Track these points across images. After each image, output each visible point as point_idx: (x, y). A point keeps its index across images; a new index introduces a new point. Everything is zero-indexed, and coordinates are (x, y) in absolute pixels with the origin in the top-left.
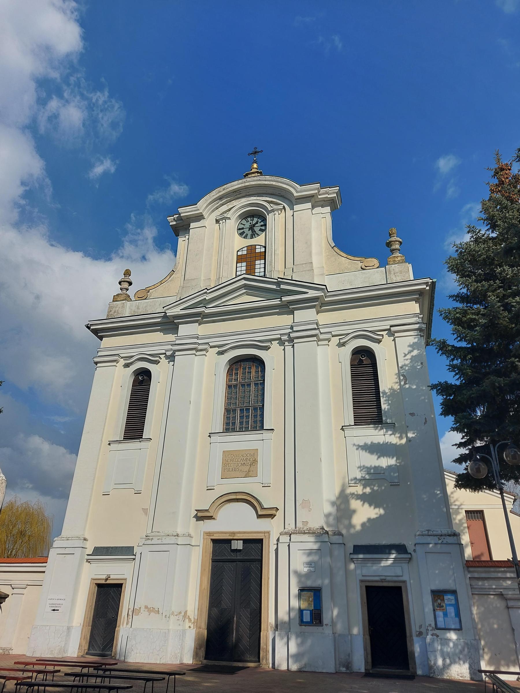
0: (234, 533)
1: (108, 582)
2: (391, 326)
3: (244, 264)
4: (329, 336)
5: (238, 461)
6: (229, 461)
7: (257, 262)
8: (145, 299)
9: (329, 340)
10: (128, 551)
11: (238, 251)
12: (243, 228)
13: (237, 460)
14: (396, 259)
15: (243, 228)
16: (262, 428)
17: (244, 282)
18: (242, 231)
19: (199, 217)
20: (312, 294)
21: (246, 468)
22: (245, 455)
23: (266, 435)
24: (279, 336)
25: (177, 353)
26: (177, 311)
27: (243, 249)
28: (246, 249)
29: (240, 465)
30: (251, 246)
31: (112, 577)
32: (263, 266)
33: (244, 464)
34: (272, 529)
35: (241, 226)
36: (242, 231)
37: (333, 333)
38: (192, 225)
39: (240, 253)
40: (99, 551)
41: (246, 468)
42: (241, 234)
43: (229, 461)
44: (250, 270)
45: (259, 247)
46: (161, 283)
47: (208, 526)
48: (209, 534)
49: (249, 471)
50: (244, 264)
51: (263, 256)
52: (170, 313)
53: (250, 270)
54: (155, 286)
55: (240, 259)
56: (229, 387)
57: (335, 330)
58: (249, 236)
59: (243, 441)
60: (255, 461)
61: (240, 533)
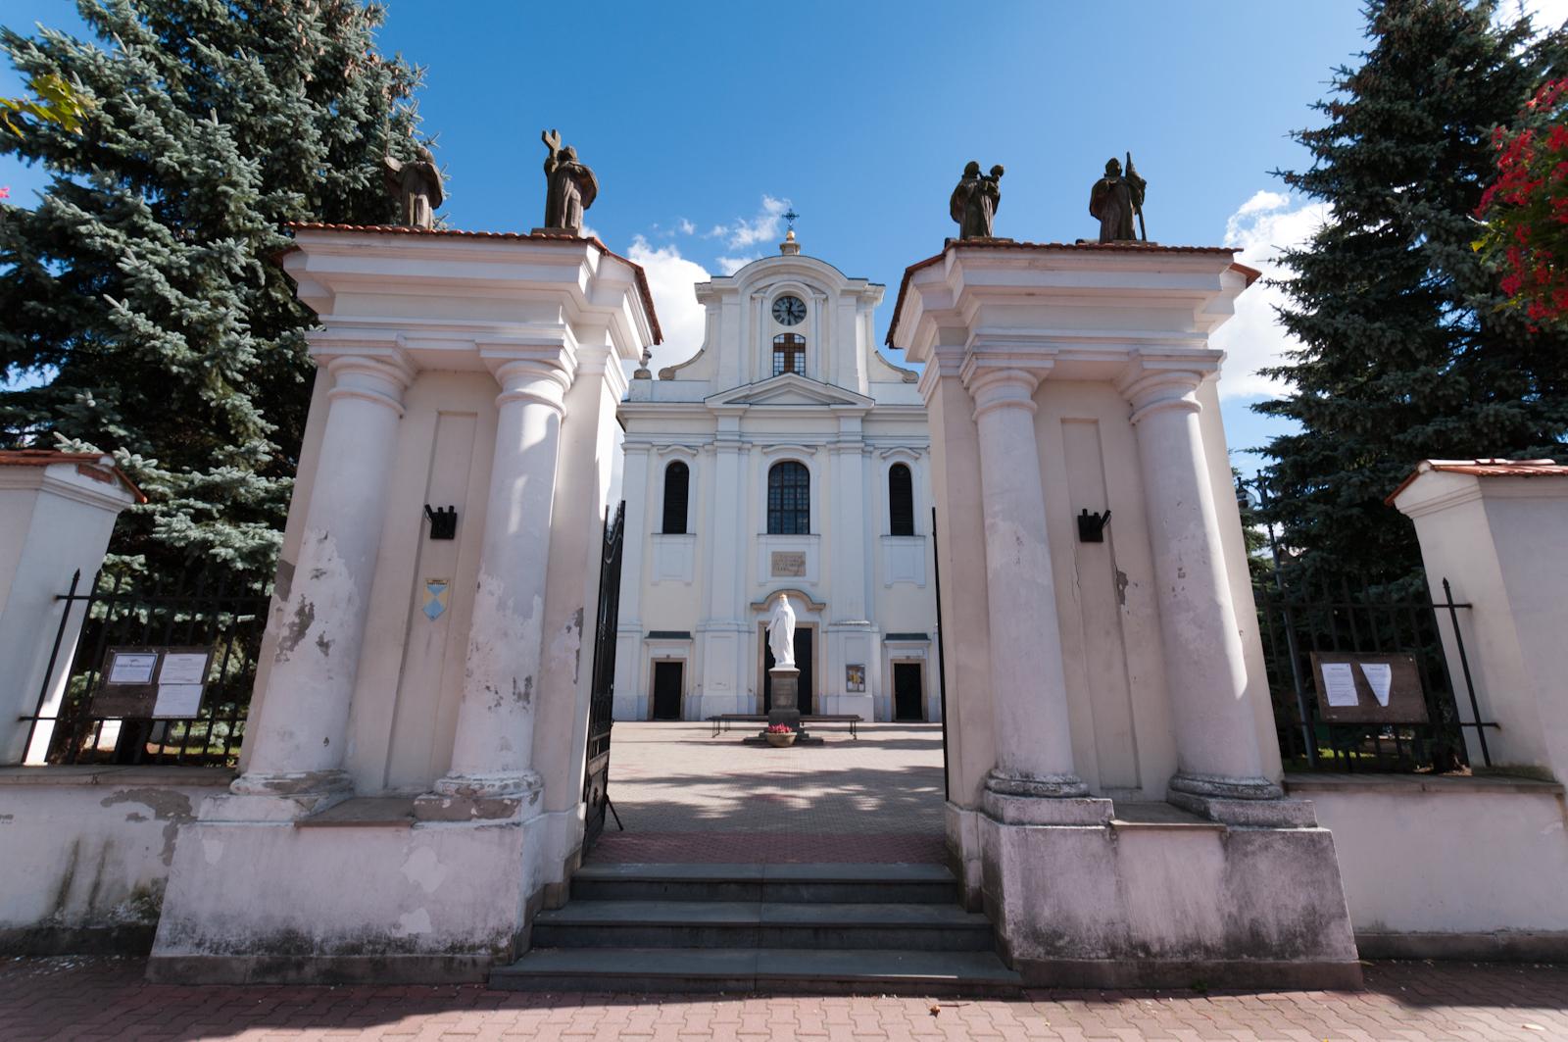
3: (782, 354)
4: (871, 449)
7: (797, 355)
9: (871, 452)
10: (685, 635)
16: (809, 533)
17: (788, 381)
19: (734, 291)
21: (796, 568)
23: (812, 539)
26: (717, 403)
33: (792, 564)
35: (777, 308)
38: (725, 299)
39: (777, 341)
40: (654, 635)
41: (796, 568)
42: (777, 318)
44: (789, 366)
46: (689, 363)
47: (763, 617)
50: (782, 354)
51: (802, 348)
52: (710, 404)
54: (682, 366)
55: (777, 348)
56: (770, 487)
57: (879, 443)
58: (786, 322)
59: (788, 543)
60: (803, 563)
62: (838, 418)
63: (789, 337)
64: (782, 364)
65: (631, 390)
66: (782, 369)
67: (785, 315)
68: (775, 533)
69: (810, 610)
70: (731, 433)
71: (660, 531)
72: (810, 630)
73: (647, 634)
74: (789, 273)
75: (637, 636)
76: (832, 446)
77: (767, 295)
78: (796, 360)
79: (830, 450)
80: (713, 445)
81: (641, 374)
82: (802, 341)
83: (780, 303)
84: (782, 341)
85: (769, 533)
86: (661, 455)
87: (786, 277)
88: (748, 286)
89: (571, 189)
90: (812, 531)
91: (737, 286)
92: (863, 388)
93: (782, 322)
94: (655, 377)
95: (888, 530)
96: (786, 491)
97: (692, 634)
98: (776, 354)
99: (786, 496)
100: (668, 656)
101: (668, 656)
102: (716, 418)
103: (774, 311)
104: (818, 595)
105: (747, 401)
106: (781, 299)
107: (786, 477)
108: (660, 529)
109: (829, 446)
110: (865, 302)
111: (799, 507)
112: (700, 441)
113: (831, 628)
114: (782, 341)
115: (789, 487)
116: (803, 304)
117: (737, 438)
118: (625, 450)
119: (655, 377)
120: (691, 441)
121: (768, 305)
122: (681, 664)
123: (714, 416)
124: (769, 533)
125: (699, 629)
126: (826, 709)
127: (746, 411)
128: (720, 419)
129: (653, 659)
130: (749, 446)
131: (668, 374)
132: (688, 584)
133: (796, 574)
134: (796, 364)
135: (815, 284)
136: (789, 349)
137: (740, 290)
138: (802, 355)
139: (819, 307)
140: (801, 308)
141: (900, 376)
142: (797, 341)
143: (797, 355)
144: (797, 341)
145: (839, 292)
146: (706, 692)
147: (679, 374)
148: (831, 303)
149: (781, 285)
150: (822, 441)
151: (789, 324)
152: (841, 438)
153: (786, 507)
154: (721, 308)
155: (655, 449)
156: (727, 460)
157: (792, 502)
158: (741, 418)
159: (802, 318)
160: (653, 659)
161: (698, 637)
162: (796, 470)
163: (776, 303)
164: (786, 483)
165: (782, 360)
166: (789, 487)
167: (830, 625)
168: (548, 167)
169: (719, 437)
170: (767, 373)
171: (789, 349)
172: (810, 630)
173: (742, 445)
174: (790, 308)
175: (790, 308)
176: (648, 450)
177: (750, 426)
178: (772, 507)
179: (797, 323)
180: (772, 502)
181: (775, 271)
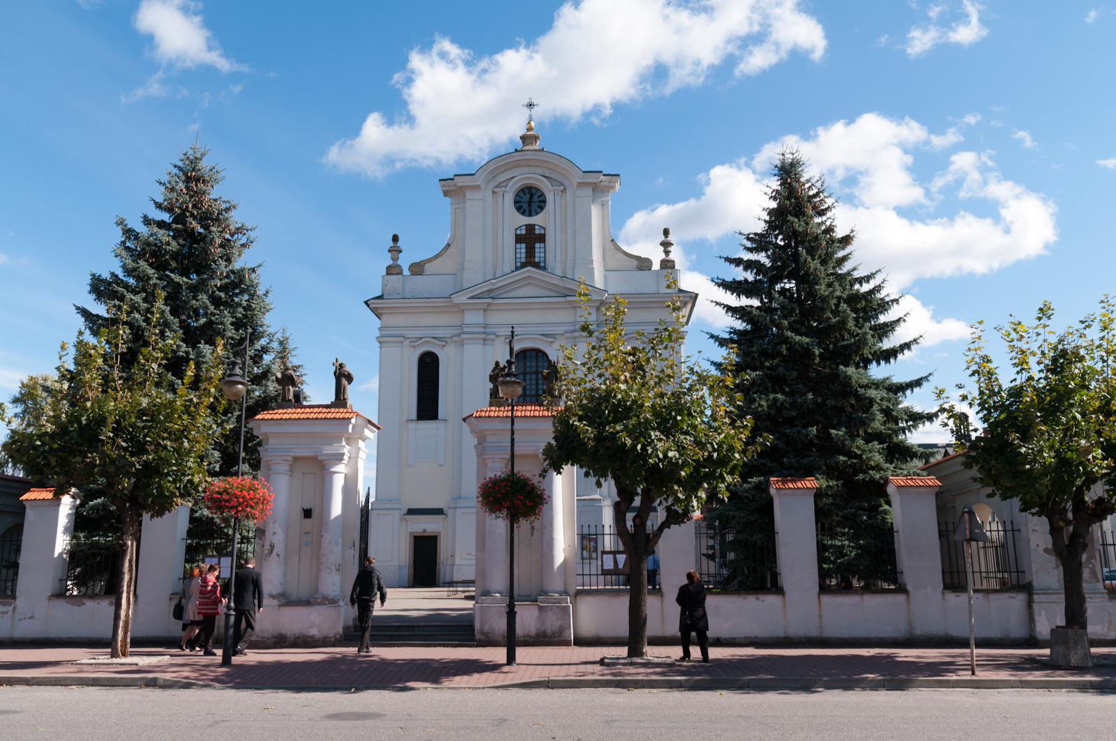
1: (426, 534)
3: (523, 245)
7: (537, 245)
8: (420, 274)
10: (439, 512)
12: (520, 202)
15: (520, 202)
19: (477, 187)
26: (462, 299)
28: (524, 228)
30: (530, 225)
32: (542, 250)
35: (518, 199)
38: (469, 195)
39: (518, 232)
40: (411, 512)
44: (530, 252)
46: (436, 257)
50: (523, 245)
51: (542, 238)
53: (530, 252)
54: (430, 260)
55: (519, 239)
63: (530, 228)
64: (524, 255)
65: (384, 286)
66: (523, 260)
70: (476, 325)
71: (414, 417)
74: (528, 166)
75: (397, 514)
76: (569, 335)
77: (507, 189)
78: (537, 250)
79: (567, 338)
80: (460, 336)
81: (392, 270)
82: (542, 232)
84: (524, 232)
87: (526, 170)
88: (489, 181)
89: (344, 382)
93: (523, 213)
94: (406, 272)
97: (445, 512)
98: (518, 246)
100: (425, 531)
101: (425, 531)
102: (463, 311)
105: (489, 297)
107: (528, 364)
108: (414, 415)
112: (448, 333)
114: (524, 232)
115: (531, 373)
117: (482, 330)
118: (380, 343)
119: (406, 272)
120: (440, 333)
121: (510, 198)
123: (461, 309)
125: (451, 506)
126: (452, 576)
127: (489, 304)
128: (466, 312)
129: (411, 533)
130: (493, 337)
131: (417, 269)
132: (441, 466)
134: (537, 255)
135: (554, 176)
136: (530, 239)
137: (482, 186)
138: (542, 245)
139: (558, 198)
141: (635, 263)
142: (537, 232)
143: (537, 245)
144: (537, 232)
145: (575, 185)
146: (458, 561)
148: (569, 195)
151: (530, 215)
154: (465, 202)
155: (407, 342)
157: (534, 387)
158: (485, 310)
161: (450, 512)
162: (537, 357)
164: (528, 370)
165: (524, 251)
166: (531, 373)
168: (335, 374)
169: (465, 330)
170: (509, 265)
171: (530, 239)
173: (486, 336)
174: (530, 200)
175: (530, 200)
176: (402, 343)
177: (495, 318)
181: (516, 165)
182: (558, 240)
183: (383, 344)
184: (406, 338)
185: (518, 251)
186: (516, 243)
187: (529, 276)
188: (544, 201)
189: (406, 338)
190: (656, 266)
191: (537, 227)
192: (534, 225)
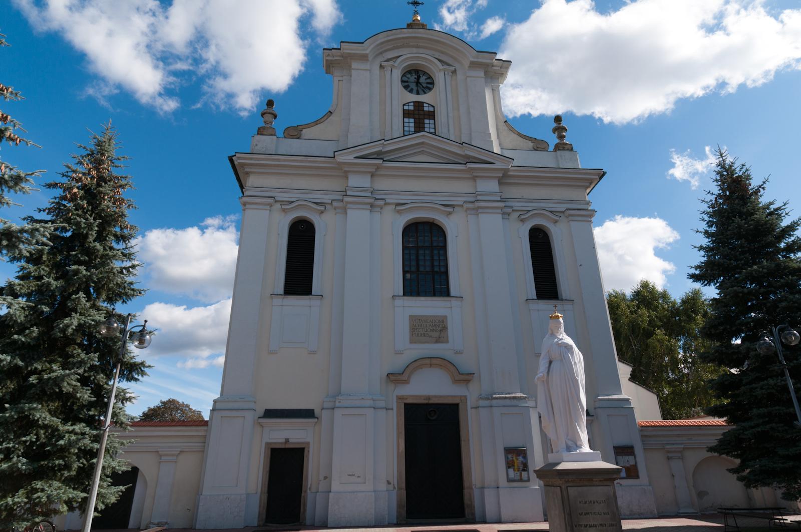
0: (429, 398)
1: (287, 446)
2: (568, 209)
3: (412, 120)
5: (426, 327)
6: (417, 326)
7: (426, 121)
8: (298, 138)
10: (308, 414)
11: (404, 105)
12: (407, 82)
13: (425, 326)
14: (566, 147)
15: (407, 82)
18: (406, 84)
19: (363, 58)
20: (498, 165)
21: (436, 334)
22: (434, 322)
23: (454, 302)
24: (461, 203)
25: (349, 206)
27: (410, 104)
28: (412, 104)
29: (429, 330)
30: (418, 102)
31: (290, 441)
32: (432, 126)
34: (470, 394)
35: (405, 79)
36: (406, 84)
37: (514, 208)
38: (355, 65)
39: (406, 108)
40: (270, 414)
41: (436, 334)
42: (406, 87)
43: (417, 326)
44: (419, 128)
45: (427, 105)
48: (399, 398)
49: (439, 337)
50: (412, 120)
55: (407, 114)
57: (517, 205)
58: (415, 91)
60: (445, 328)
61: (435, 397)
62: (474, 179)
63: (419, 105)
67: (413, 86)
68: (411, 295)
69: (456, 381)
70: (363, 189)
72: (457, 405)
73: (261, 412)
74: (418, 47)
75: (250, 417)
76: (470, 206)
77: (396, 64)
78: (426, 126)
79: (468, 209)
80: (342, 202)
82: (431, 109)
83: (409, 76)
84: (412, 108)
85: (404, 295)
86: (284, 210)
87: (415, 50)
90: (453, 292)
91: (367, 52)
92: (496, 149)
93: (411, 91)
95: (533, 293)
96: (421, 252)
97: (317, 412)
98: (406, 120)
99: (421, 257)
100: (287, 441)
101: (287, 441)
103: (402, 81)
104: (466, 363)
105: (379, 158)
106: (410, 72)
108: (281, 289)
109: (466, 205)
110: (492, 78)
111: (436, 269)
113: (482, 403)
114: (412, 108)
116: (430, 77)
117: (369, 194)
119: (280, 133)
120: (319, 197)
121: (397, 74)
122: (303, 449)
123: (344, 171)
124: (404, 295)
125: (326, 405)
127: (378, 167)
129: (267, 444)
130: (382, 203)
131: (294, 133)
132: (313, 353)
133: (438, 341)
136: (419, 116)
137: (370, 58)
138: (432, 122)
139: (448, 79)
140: (429, 81)
141: (530, 144)
142: (426, 109)
143: (426, 121)
144: (426, 109)
145: (466, 64)
146: (335, 486)
147: (306, 132)
148: (460, 76)
149: (408, 57)
150: (459, 200)
151: (418, 93)
152: (479, 198)
153: (422, 269)
155: (278, 205)
156: (358, 217)
157: (428, 263)
158: (372, 176)
159: (430, 89)
160: (267, 444)
161: (325, 415)
163: (404, 75)
165: (412, 125)
167: (481, 399)
169: (348, 193)
170: (398, 131)
171: (419, 116)
172: (457, 405)
173: (375, 202)
175: (417, 79)
176: (271, 206)
177: (383, 184)
178: (407, 269)
179: (425, 93)
180: (407, 263)
181: (404, 43)
182: (451, 115)
183: (247, 206)
184: (276, 201)
185: (406, 124)
186: (404, 118)
187: (423, 143)
188: (433, 83)
189: (276, 201)
190: (551, 148)
191: (425, 105)
192: (423, 103)
